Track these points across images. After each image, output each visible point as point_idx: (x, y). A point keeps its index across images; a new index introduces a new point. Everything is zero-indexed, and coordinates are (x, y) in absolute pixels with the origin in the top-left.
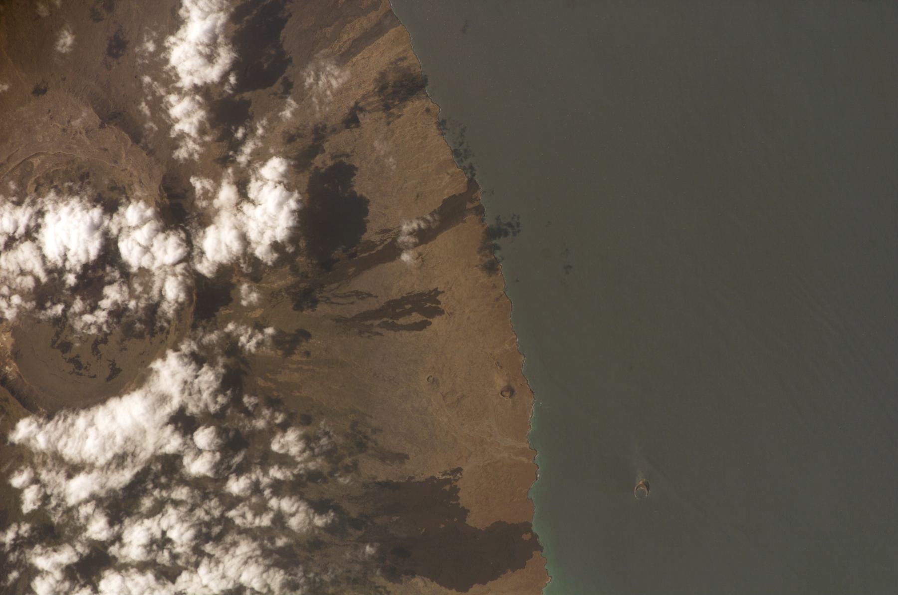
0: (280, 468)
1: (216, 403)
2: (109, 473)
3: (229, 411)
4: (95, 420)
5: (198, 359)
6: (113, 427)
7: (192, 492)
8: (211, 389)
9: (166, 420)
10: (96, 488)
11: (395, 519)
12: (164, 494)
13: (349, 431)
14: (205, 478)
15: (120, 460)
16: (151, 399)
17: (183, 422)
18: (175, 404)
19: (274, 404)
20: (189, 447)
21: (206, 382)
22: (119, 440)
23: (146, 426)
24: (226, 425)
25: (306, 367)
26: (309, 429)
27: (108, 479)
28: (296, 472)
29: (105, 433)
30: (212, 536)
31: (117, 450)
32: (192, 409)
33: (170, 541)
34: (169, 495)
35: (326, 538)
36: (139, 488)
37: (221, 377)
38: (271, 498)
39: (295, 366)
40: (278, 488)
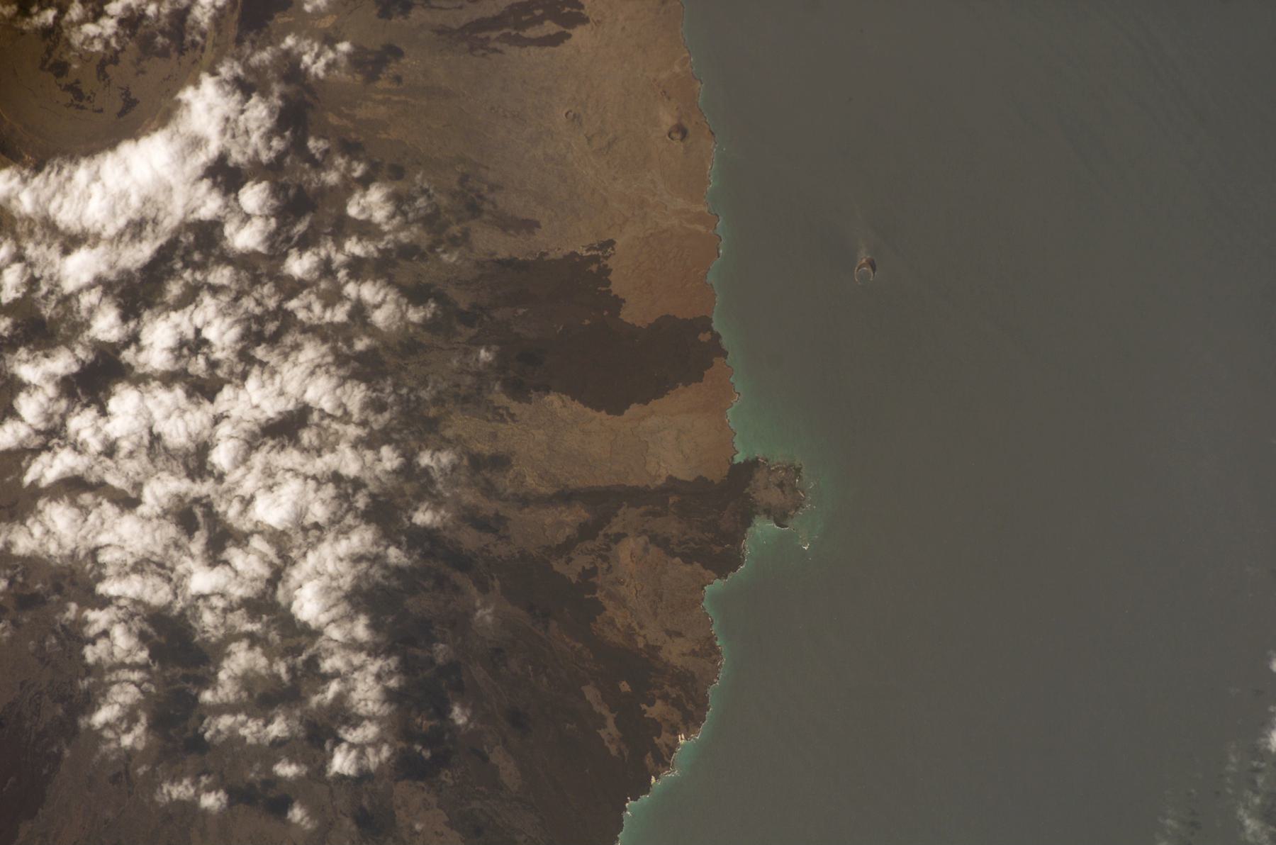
0: (360, 240)
1: (270, 148)
2: (121, 247)
3: (288, 160)
4: (101, 173)
5: (245, 87)
6: (127, 182)
7: (238, 274)
8: (263, 129)
9: (200, 172)
10: (103, 268)
11: (521, 311)
12: (199, 276)
13: (457, 188)
14: (254, 254)
15: (136, 229)
16: (178, 143)
17: (225, 175)
18: (213, 149)
19: (351, 149)
20: (232, 211)
21: (257, 119)
22: (135, 201)
23: (173, 181)
24: (284, 179)
25: (396, 98)
26: (400, 185)
27: (120, 255)
28: (381, 245)
29: (116, 190)
30: (265, 335)
31: (132, 214)
32: (237, 157)
33: (206, 342)
34: (205, 279)
35: (425, 337)
36: (163, 268)
37: (278, 111)
38: (347, 282)
39: (380, 97)
40: (357, 268)
